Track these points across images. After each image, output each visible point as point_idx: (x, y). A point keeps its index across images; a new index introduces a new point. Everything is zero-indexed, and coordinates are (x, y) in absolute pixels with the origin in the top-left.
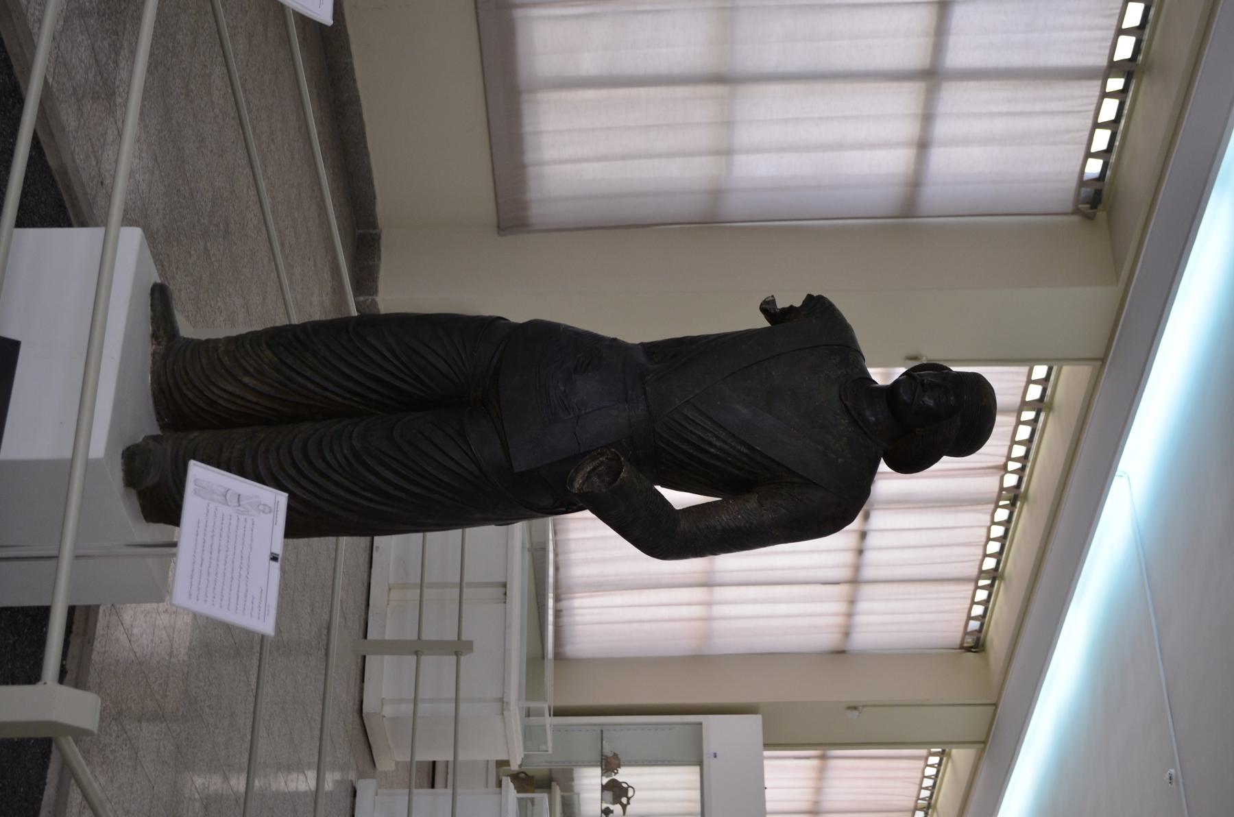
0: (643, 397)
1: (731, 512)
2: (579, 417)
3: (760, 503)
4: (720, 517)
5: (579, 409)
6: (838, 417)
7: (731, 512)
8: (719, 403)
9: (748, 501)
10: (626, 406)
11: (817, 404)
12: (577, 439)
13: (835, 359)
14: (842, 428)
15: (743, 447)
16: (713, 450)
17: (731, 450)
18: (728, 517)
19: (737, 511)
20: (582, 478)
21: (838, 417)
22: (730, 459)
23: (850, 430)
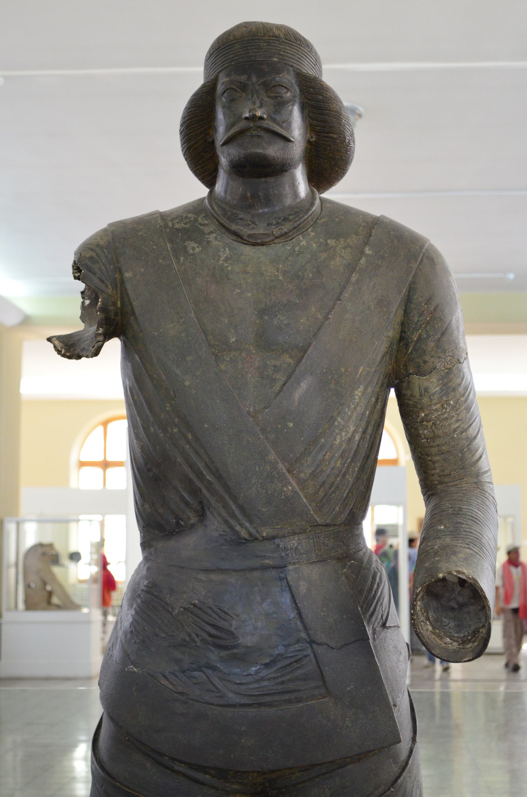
0: (277, 541)
1: (446, 415)
2: (312, 642)
3: (431, 372)
4: (455, 431)
5: (298, 641)
6: (297, 249)
7: (446, 415)
8: (291, 425)
9: (426, 390)
10: (290, 567)
11: (281, 278)
12: (348, 644)
13: (193, 249)
14: (314, 245)
15: (356, 392)
16: (357, 437)
17: (359, 408)
18: (454, 419)
19: (442, 406)
20: (441, 638)
21: (297, 249)
22: (367, 412)
23: (313, 234)
